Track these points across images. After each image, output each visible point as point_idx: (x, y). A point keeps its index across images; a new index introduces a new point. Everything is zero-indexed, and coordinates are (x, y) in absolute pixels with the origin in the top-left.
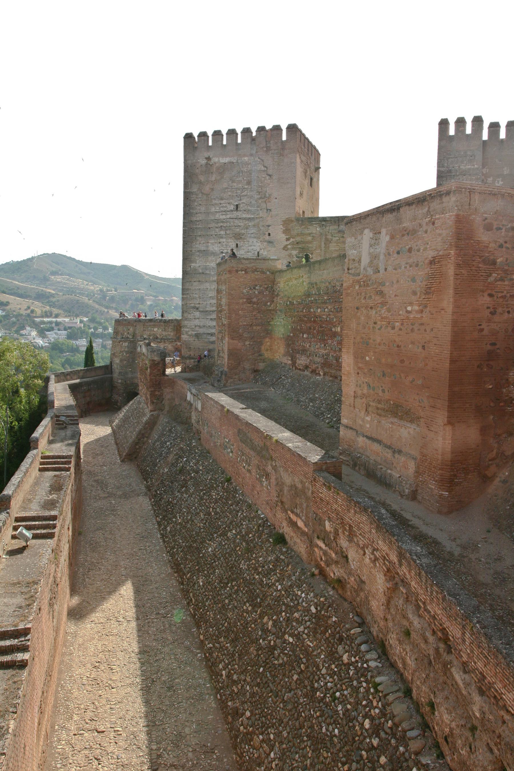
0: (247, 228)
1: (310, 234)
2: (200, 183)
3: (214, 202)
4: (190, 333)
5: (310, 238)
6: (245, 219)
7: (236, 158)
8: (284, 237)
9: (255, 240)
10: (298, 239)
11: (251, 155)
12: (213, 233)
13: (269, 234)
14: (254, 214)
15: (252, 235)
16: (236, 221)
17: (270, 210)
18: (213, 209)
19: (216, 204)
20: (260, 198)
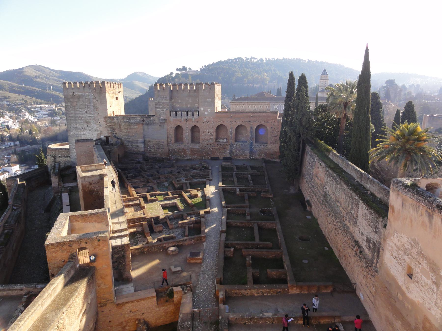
0: (91, 120)
1: (114, 123)
2: (71, 102)
3: (77, 109)
4: (73, 158)
5: (114, 124)
6: (90, 116)
7: (84, 93)
8: (105, 123)
9: (94, 124)
10: (110, 124)
11: (89, 92)
12: (78, 121)
13: (99, 122)
14: (93, 115)
15: (93, 123)
16: (86, 117)
17: (99, 113)
18: (77, 112)
19: (78, 110)
20: (95, 109)
